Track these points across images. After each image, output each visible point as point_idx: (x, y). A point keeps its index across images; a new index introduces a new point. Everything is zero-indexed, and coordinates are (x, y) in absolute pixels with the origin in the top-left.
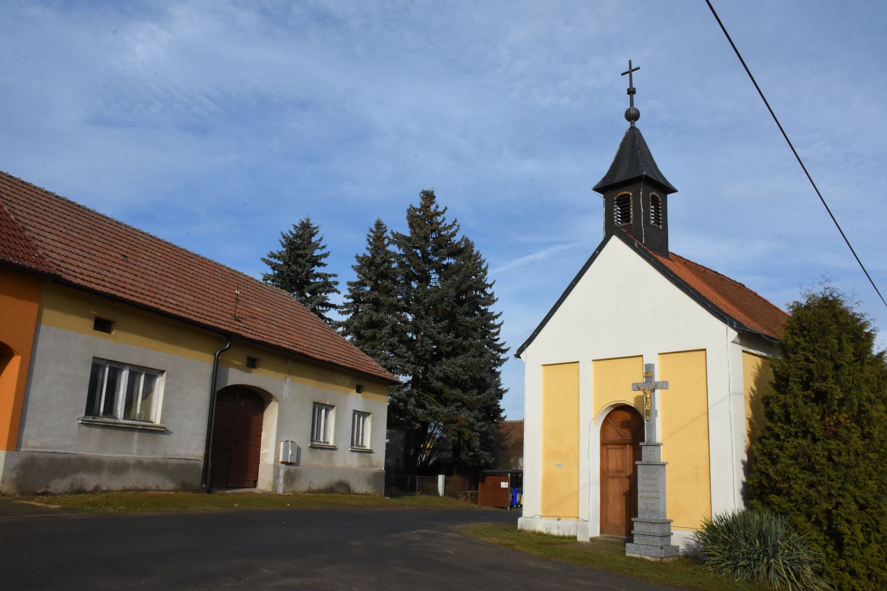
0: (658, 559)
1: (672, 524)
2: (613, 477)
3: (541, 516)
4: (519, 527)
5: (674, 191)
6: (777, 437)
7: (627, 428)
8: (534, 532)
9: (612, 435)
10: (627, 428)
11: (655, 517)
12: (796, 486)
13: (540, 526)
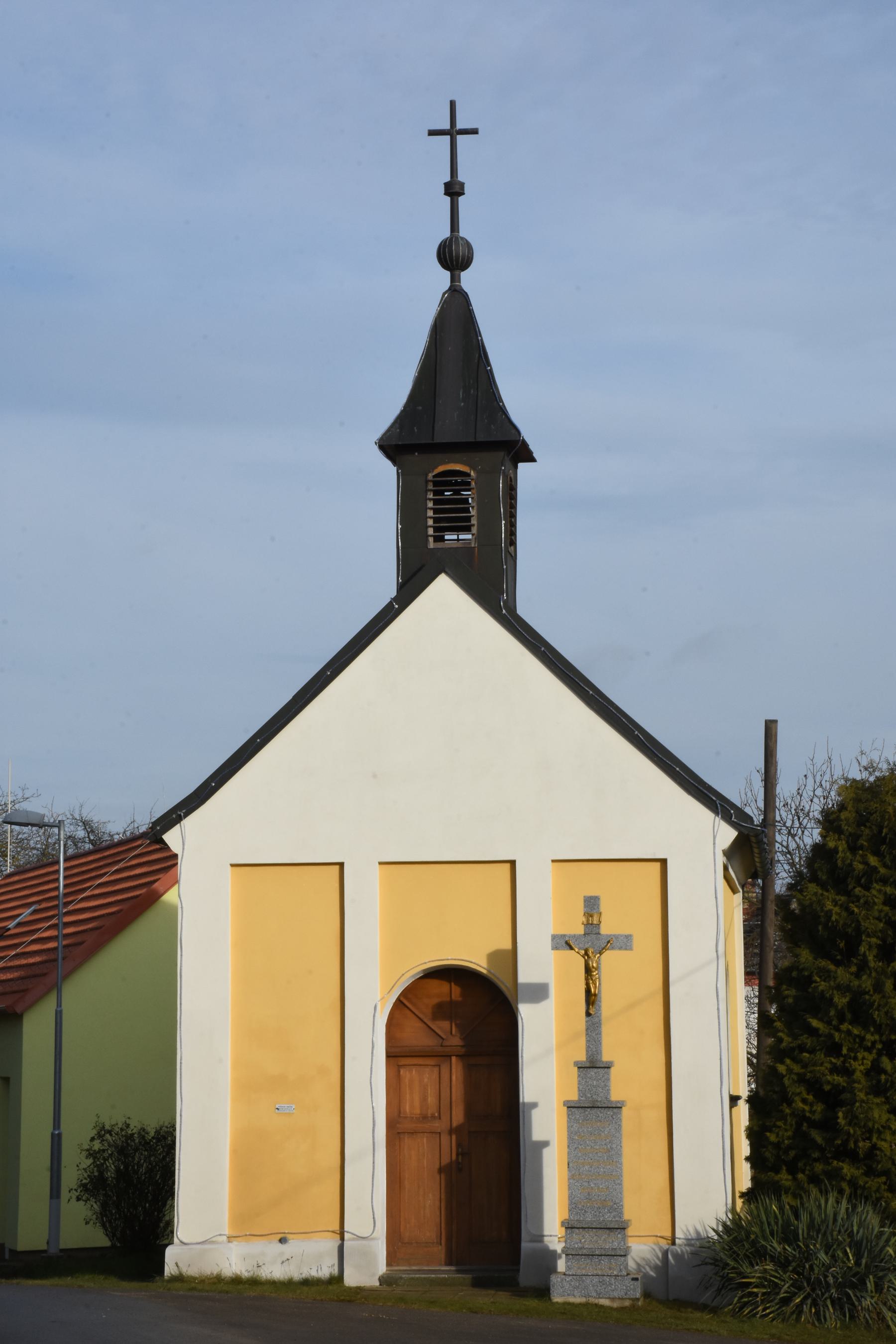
0: (627, 1303)
1: (630, 1231)
2: (413, 1133)
3: (230, 1238)
4: (170, 1269)
5: (531, 459)
6: (834, 1049)
7: (464, 1020)
8: (218, 1279)
9: (415, 1035)
10: (464, 1020)
11: (608, 1217)
12: (883, 1143)
13: (234, 1260)
